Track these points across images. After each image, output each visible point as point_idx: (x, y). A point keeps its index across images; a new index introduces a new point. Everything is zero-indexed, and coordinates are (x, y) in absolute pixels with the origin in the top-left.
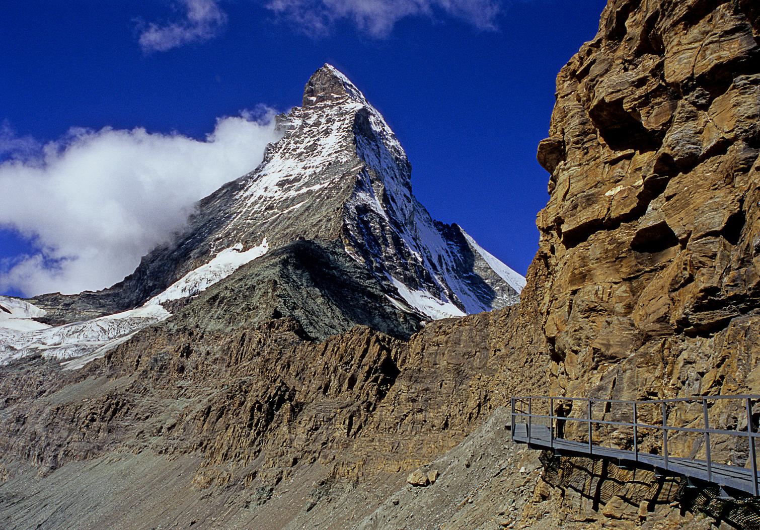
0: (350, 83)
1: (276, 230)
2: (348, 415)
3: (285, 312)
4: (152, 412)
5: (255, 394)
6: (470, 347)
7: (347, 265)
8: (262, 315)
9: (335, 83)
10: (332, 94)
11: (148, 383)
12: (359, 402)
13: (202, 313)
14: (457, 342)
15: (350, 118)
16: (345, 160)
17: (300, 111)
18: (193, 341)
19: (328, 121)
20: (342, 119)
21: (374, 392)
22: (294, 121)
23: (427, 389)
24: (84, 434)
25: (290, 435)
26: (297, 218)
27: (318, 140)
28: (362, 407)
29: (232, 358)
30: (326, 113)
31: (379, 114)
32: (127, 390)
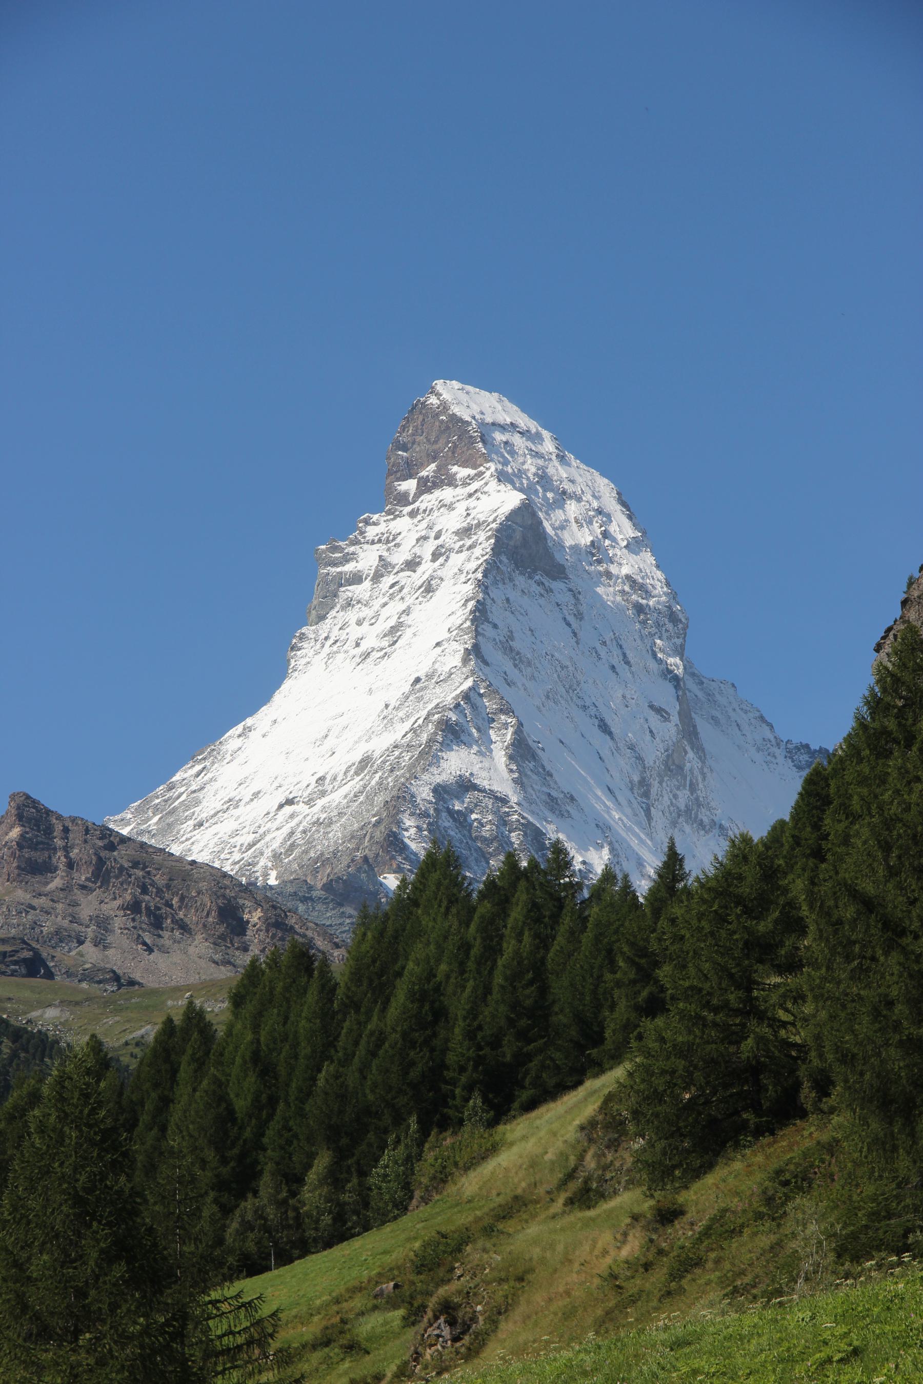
7: (329, 914)
9: (460, 438)
10: (455, 469)
15: (488, 538)
16: (446, 669)
17: (380, 526)
19: (435, 556)
20: (468, 542)
22: (362, 555)
27: (407, 611)
30: (436, 529)
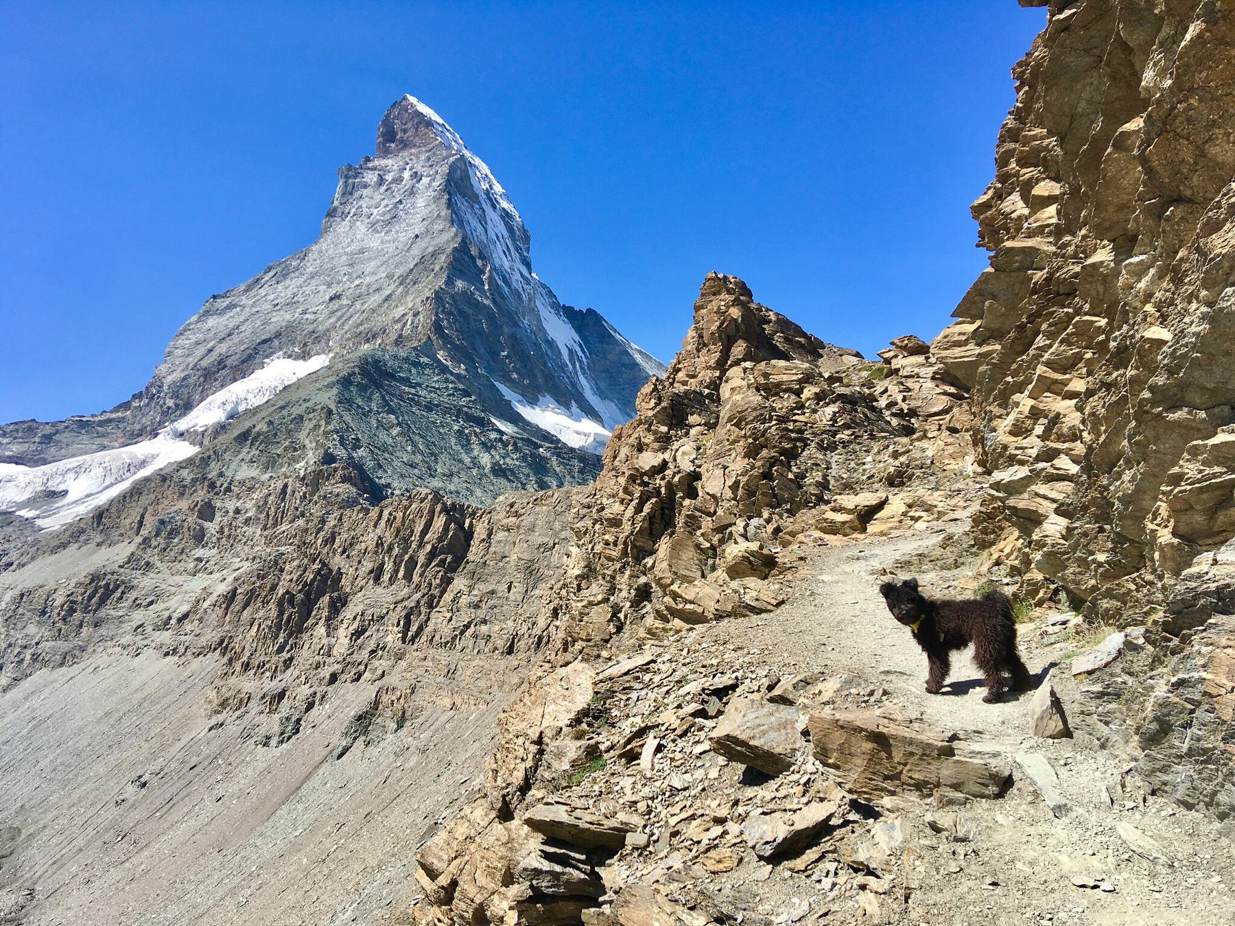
0: (441, 121)
1: (346, 328)
2: (403, 614)
3: (341, 453)
4: (157, 596)
5: (288, 578)
6: (546, 535)
8: (308, 462)
11: (152, 556)
12: (419, 595)
13: (227, 456)
14: (532, 529)
18: (217, 494)
21: (438, 581)
23: (493, 592)
24: (60, 630)
25: (327, 640)
26: (373, 311)
28: (422, 603)
29: (270, 518)
31: (484, 164)
32: (120, 567)
